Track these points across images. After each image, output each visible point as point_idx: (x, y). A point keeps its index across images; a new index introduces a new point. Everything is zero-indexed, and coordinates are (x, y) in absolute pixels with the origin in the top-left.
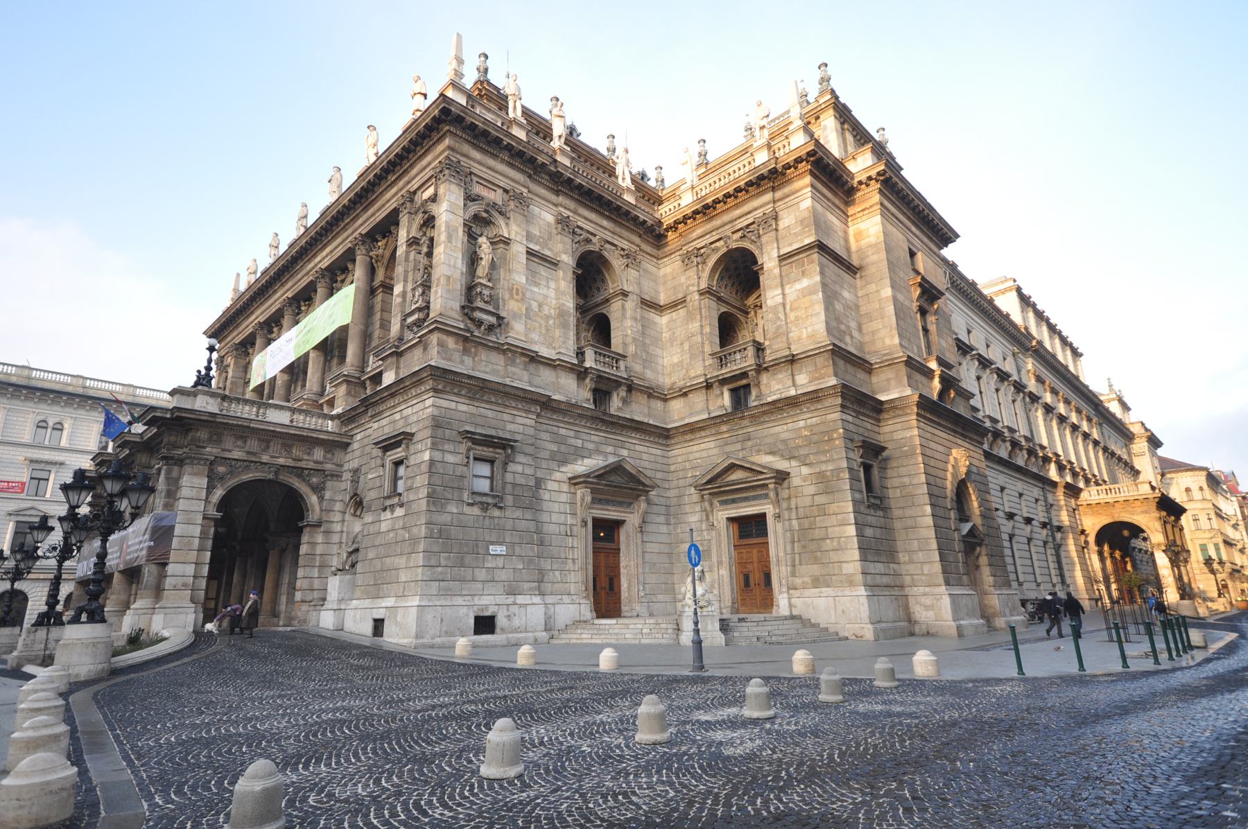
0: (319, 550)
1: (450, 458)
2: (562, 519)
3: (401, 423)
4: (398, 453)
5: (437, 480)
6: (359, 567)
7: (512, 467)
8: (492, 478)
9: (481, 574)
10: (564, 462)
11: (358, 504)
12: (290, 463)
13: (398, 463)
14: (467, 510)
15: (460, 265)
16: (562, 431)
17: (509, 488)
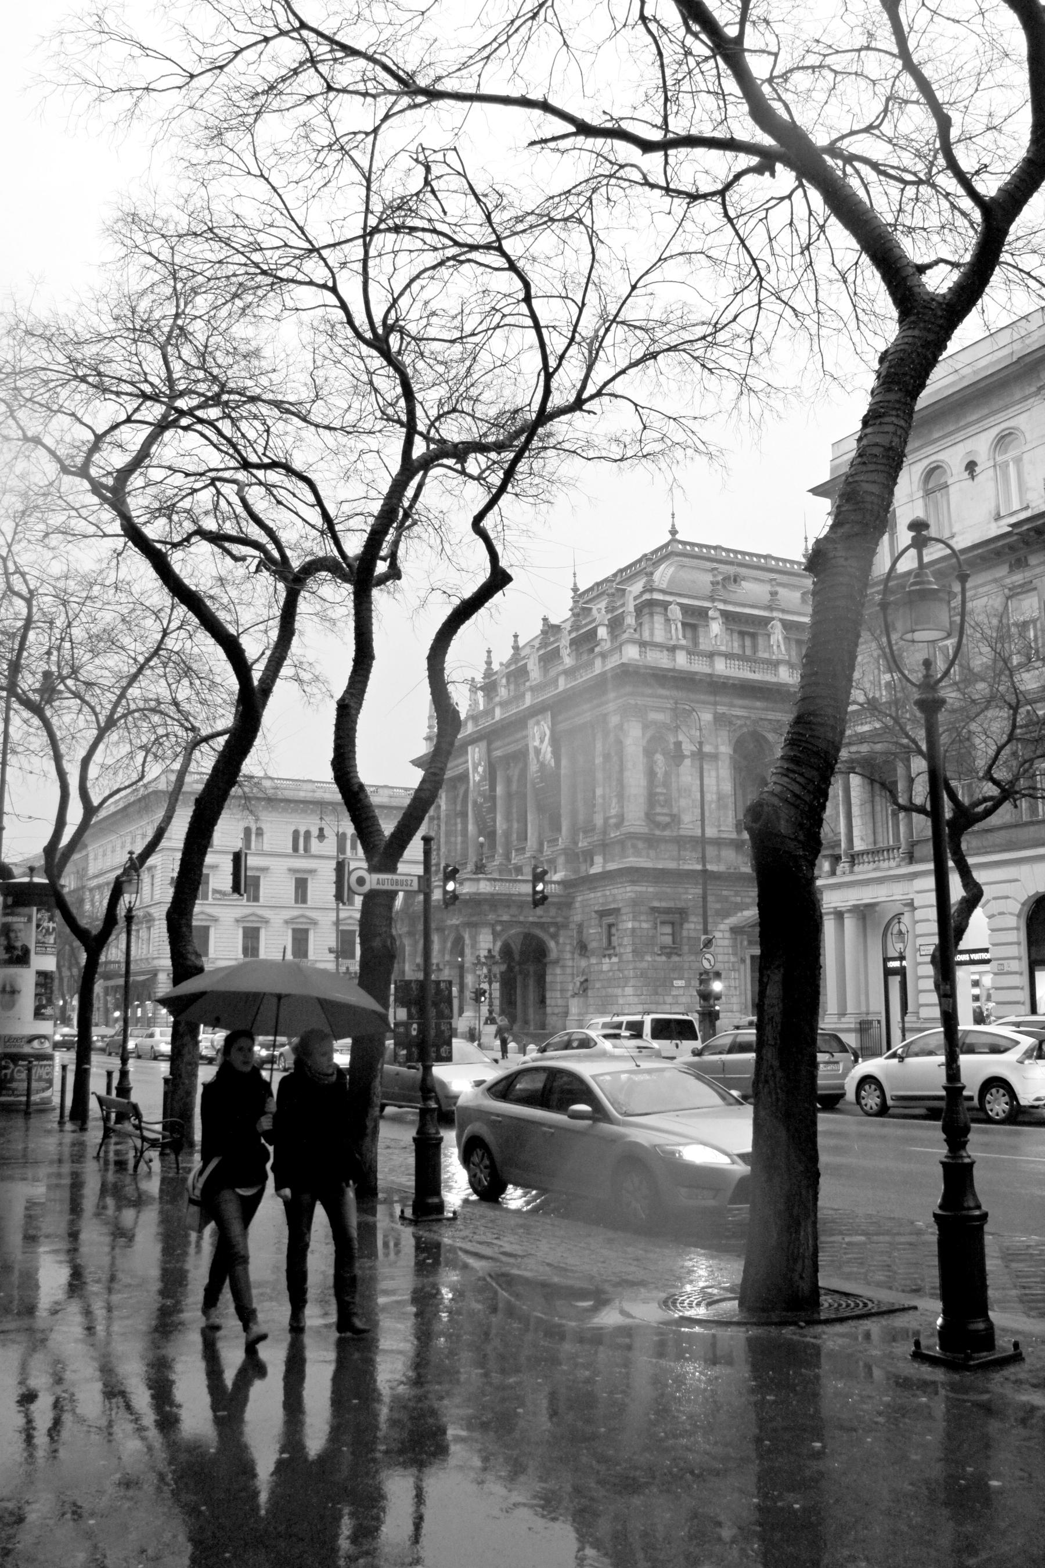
0: (559, 979)
1: (645, 925)
2: (726, 958)
3: (610, 899)
4: (611, 920)
5: (637, 941)
6: (590, 993)
7: (686, 926)
8: (673, 934)
9: (669, 999)
10: (726, 914)
11: (583, 948)
12: (536, 920)
13: (610, 926)
14: (658, 958)
15: (643, 782)
16: (725, 893)
17: (685, 940)
